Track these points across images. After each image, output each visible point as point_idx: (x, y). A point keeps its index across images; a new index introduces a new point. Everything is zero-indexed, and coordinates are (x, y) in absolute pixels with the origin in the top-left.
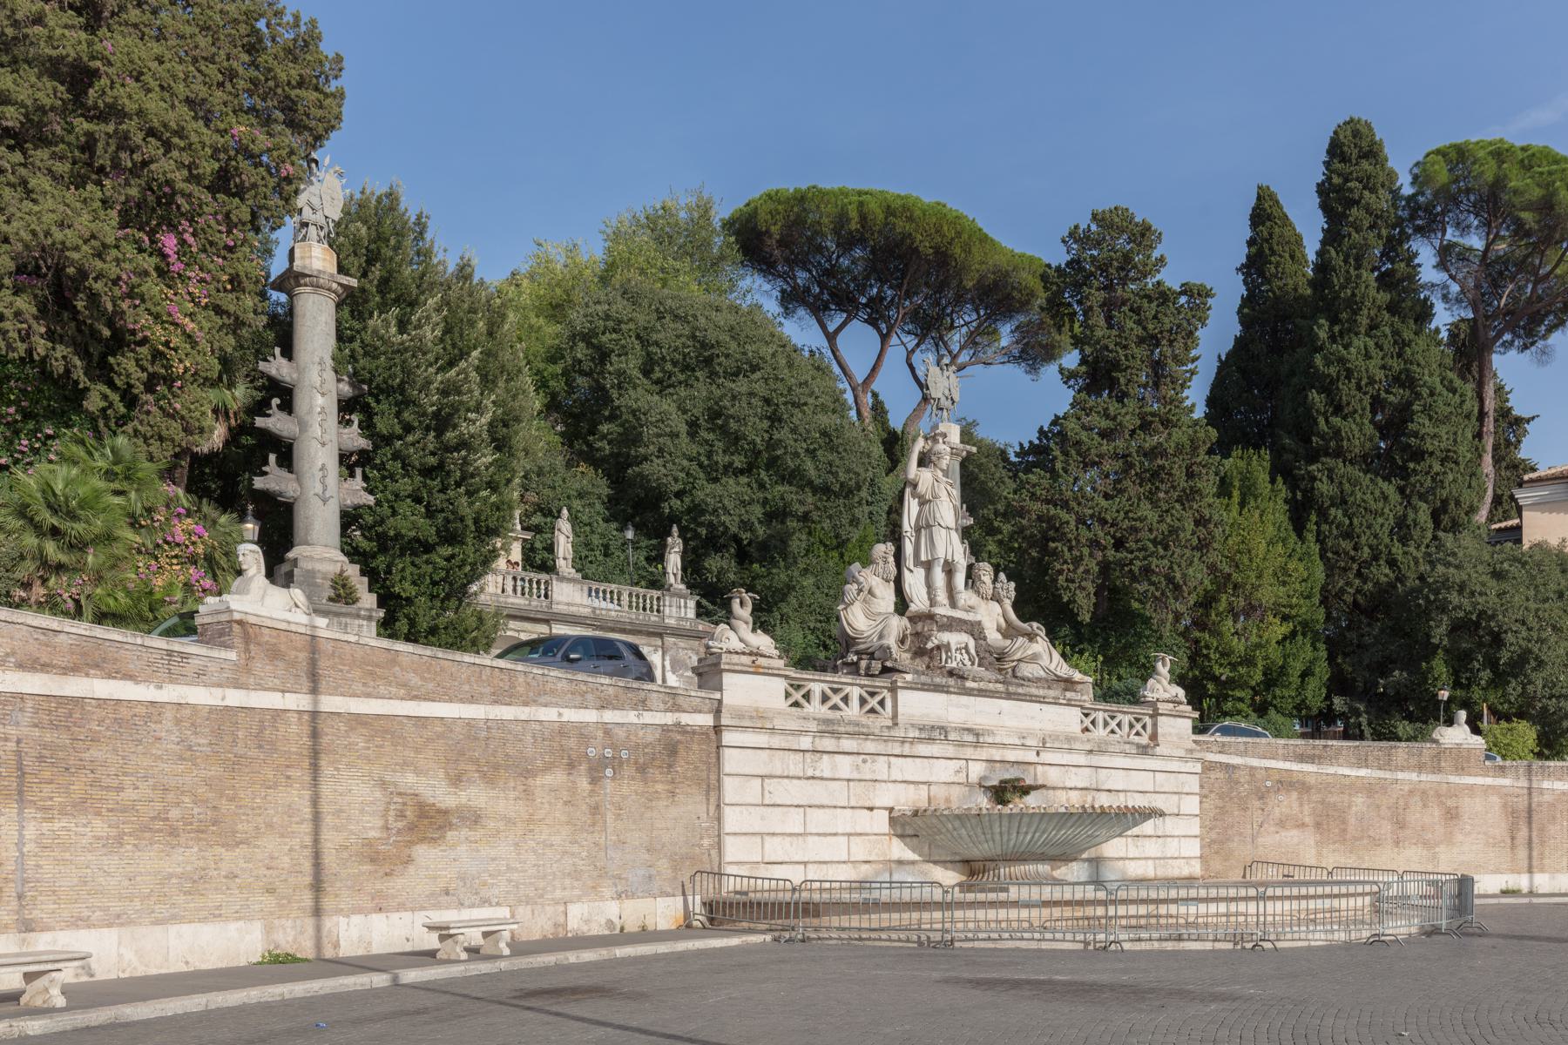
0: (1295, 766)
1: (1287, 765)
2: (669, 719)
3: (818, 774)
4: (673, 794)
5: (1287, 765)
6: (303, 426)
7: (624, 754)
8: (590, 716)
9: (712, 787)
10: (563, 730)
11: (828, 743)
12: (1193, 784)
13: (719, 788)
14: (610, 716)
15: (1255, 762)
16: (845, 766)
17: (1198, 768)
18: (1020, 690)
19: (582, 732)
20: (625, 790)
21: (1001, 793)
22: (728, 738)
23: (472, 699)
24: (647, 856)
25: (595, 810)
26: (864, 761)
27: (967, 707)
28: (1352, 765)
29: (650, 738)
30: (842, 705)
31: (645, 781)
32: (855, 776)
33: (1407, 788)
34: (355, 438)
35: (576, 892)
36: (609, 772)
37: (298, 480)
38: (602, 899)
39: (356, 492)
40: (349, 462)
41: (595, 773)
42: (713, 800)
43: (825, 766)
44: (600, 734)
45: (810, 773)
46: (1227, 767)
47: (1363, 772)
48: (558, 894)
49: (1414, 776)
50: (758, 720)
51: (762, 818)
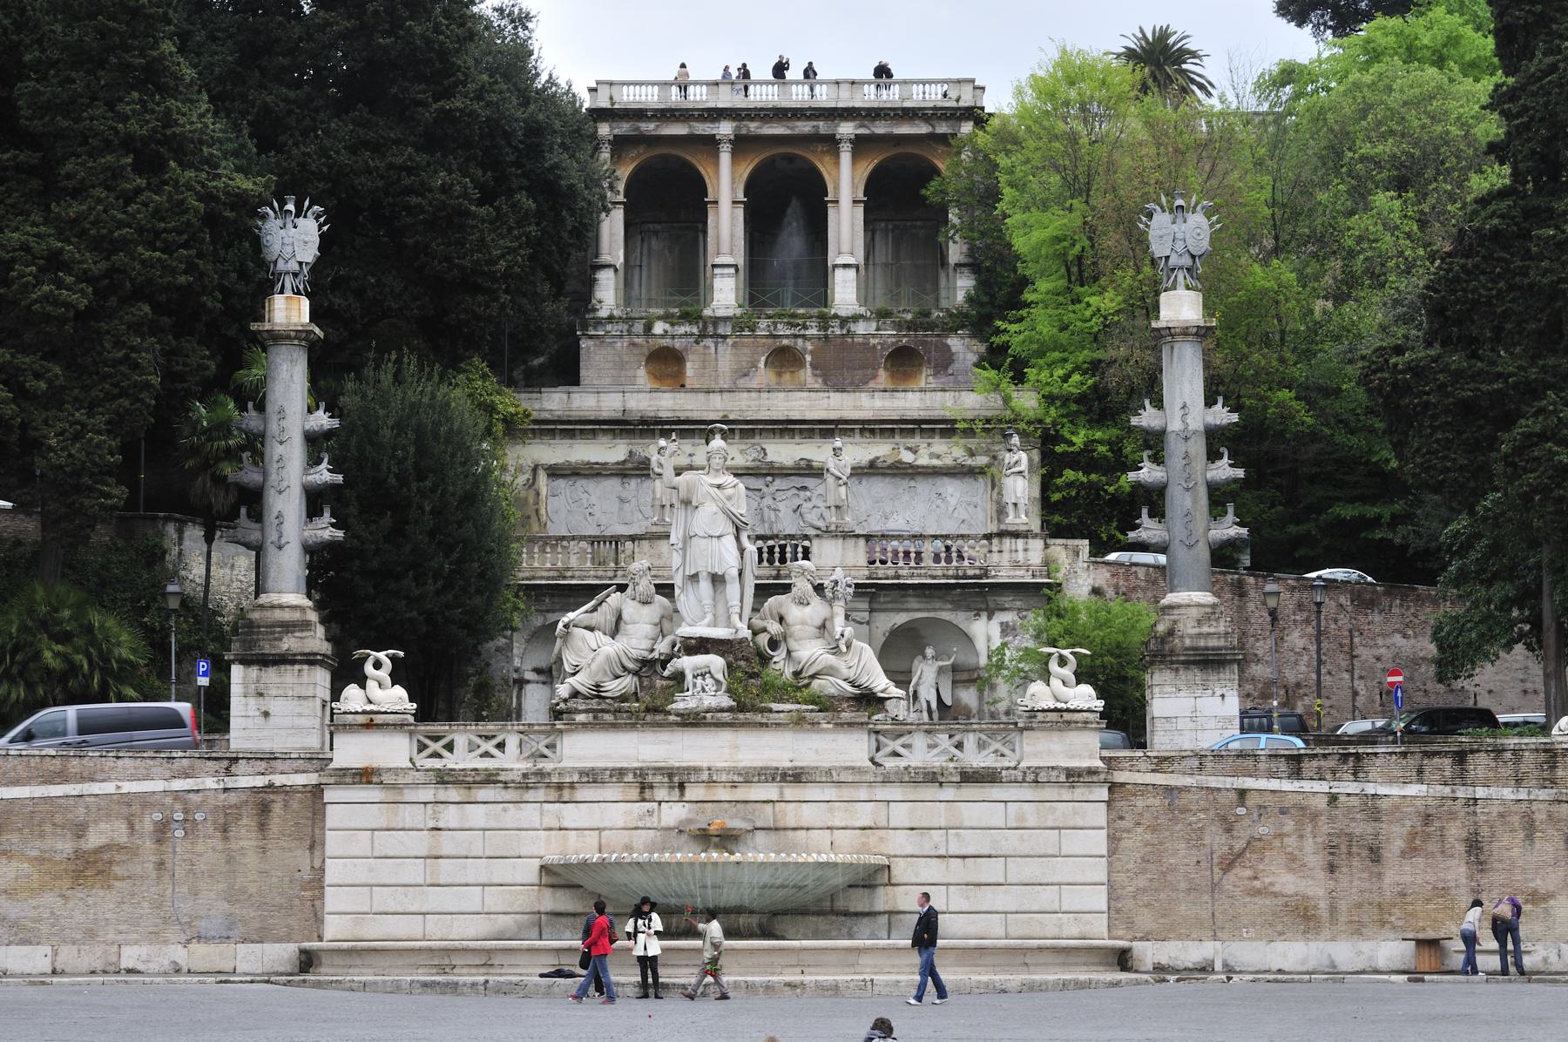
0: (1287, 786)
1: (1274, 784)
2: (260, 781)
3: (441, 825)
4: (264, 850)
5: (1274, 784)
6: (265, 474)
7: (199, 817)
8: (158, 786)
9: (315, 845)
10: (126, 800)
11: (453, 794)
12: (1099, 815)
13: (323, 844)
14: (178, 785)
15: (1213, 782)
16: (477, 815)
17: (1103, 793)
18: (759, 718)
19: (146, 801)
20: (200, 848)
21: (704, 838)
22: (329, 795)
23: (16, 782)
24: (226, 906)
25: (161, 865)
26: (505, 810)
27: (669, 743)
28: (1391, 781)
29: (233, 798)
30: (495, 751)
31: (226, 839)
32: (495, 825)
33: (1495, 810)
34: (323, 474)
35: (135, 936)
36: (179, 833)
37: (262, 530)
38: (166, 942)
39: (325, 530)
40: (315, 500)
41: (162, 831)
42: (317, 853)
43: (450, 816)
44: (168, 800)
45: (431, 824)
46: (1169, 790)
47: (1413, 790)
48: (111, 936)
49: (1508, 793)
50: (365, 776)
51: (371, 870)
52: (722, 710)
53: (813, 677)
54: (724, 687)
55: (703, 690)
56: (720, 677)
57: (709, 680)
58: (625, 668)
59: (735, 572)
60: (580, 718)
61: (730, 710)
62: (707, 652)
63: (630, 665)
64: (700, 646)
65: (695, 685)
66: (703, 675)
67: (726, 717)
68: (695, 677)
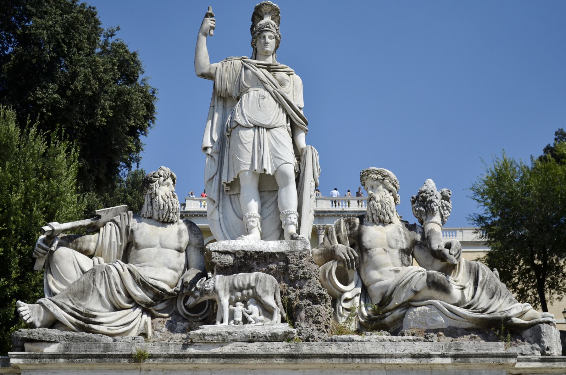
52: (274, 338)
53: (407, 305)
54: (277, 317)
55: (245, 321)
56: (269, 300)
57: (254, 309)
58: (130, 298)
59: (290, 170)
60: (52, 349)
61: (286, 337)
62: (250, 270)
63: (138, 293)
64: (246, 261)
65: (232, 315)
66: (245, 302)
67: (280, 347)
68: (232, 303)
